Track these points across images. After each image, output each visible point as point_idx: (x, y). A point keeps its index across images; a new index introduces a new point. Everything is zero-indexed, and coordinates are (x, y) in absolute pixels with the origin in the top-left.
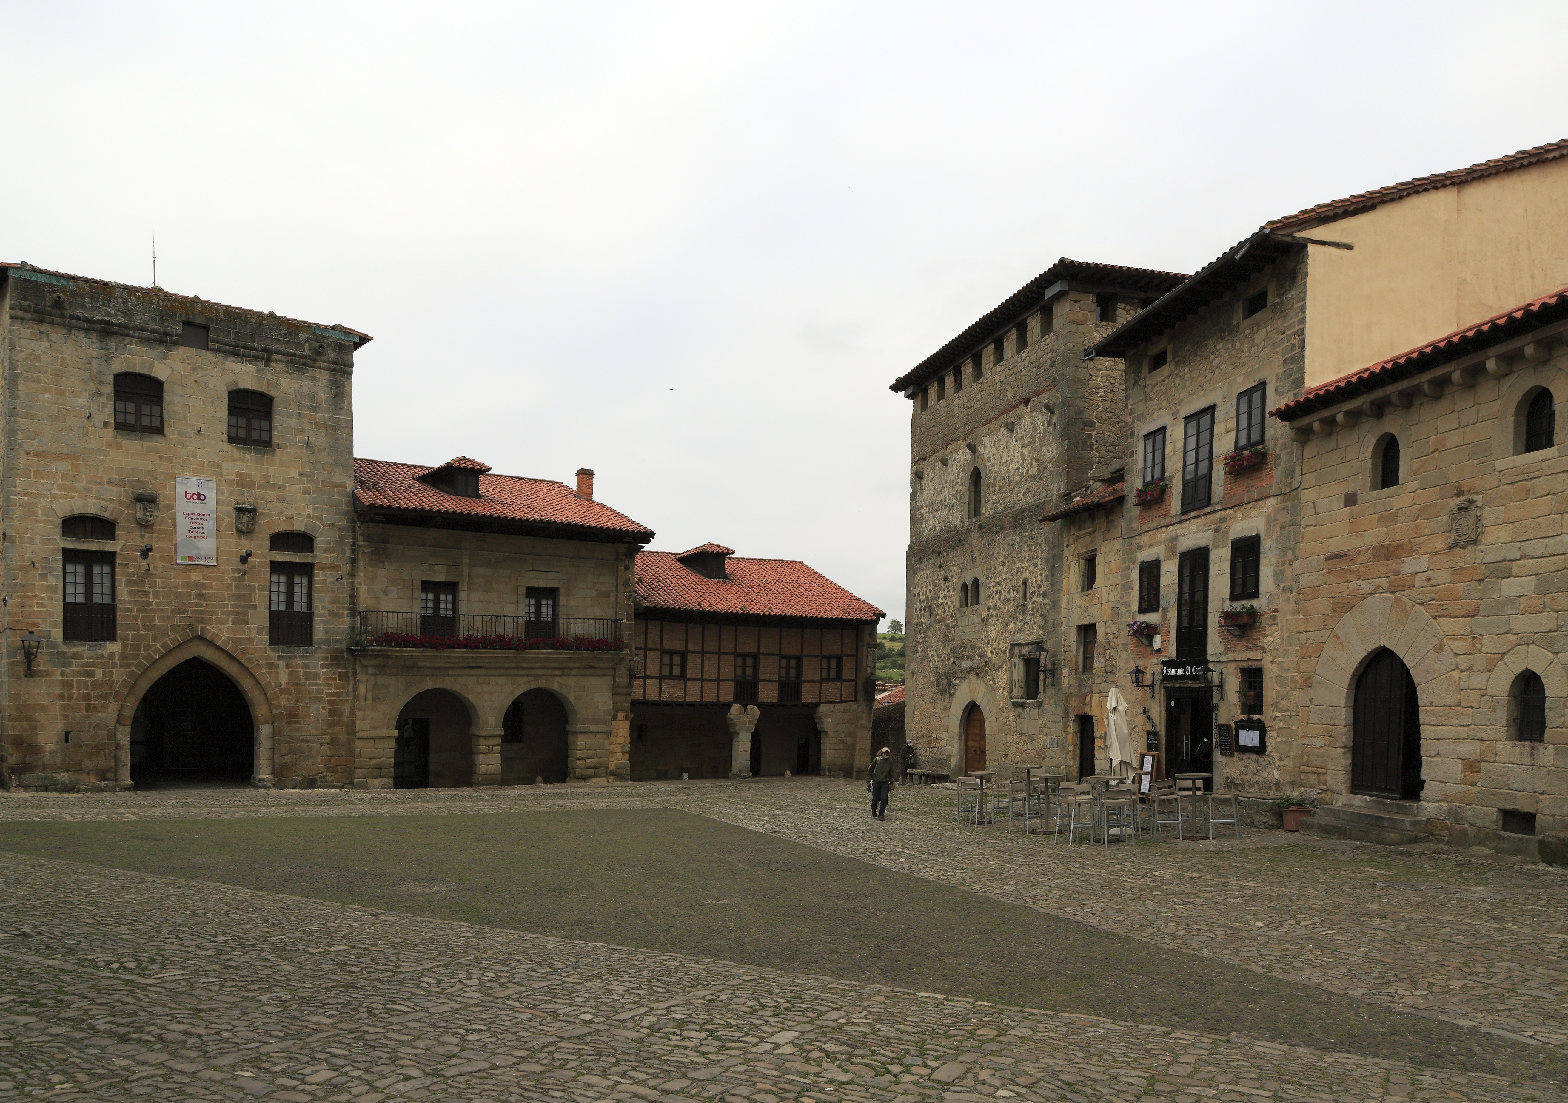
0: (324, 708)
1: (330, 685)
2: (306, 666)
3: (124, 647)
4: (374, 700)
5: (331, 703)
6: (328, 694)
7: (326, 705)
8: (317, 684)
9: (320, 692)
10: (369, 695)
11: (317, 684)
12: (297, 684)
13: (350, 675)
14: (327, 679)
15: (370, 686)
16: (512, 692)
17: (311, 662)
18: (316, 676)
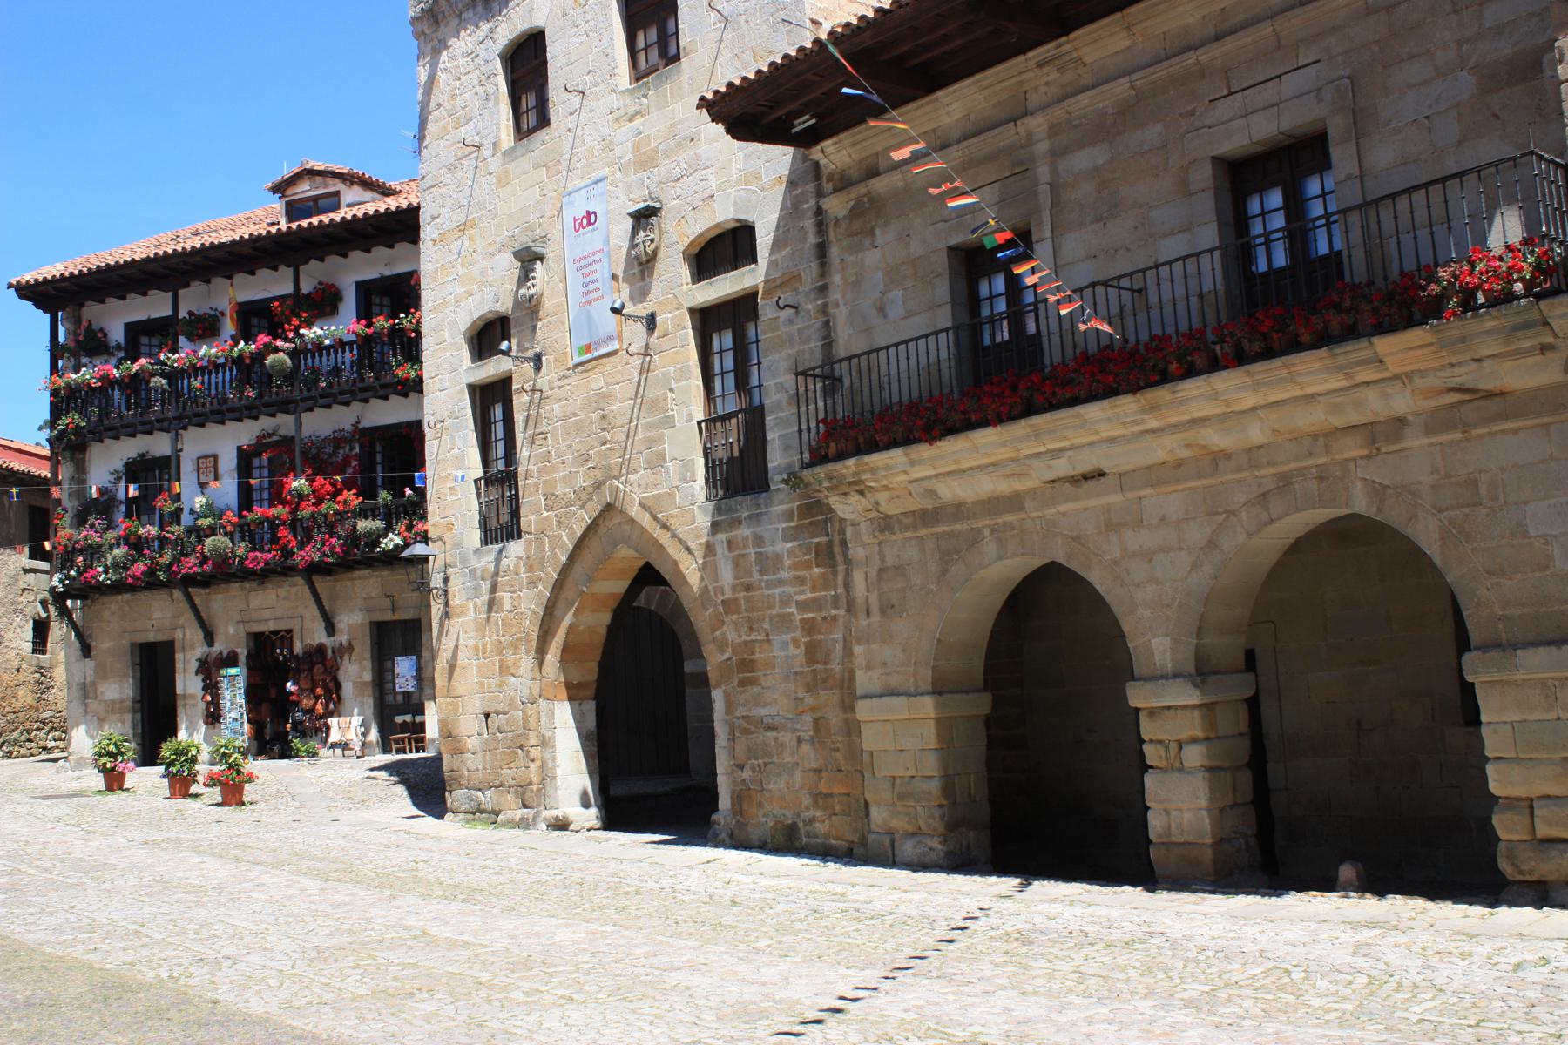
0: (795, 641)
1: (800, 581)
2: (759, 540)
3: (528, 543)
4: (883, 612)
5: (809, 627)
6: (803, 606)
7: (799, 633)
8: (781, 582)
9: (786, 600)
10: (874, 598)
11: (781, 582)
12: (748, 588)
13: (837, 549)
14: (795, 567)
15: (873, 573)
16: (1212, 544)
17: (765, 529)
18: (778, 558)
